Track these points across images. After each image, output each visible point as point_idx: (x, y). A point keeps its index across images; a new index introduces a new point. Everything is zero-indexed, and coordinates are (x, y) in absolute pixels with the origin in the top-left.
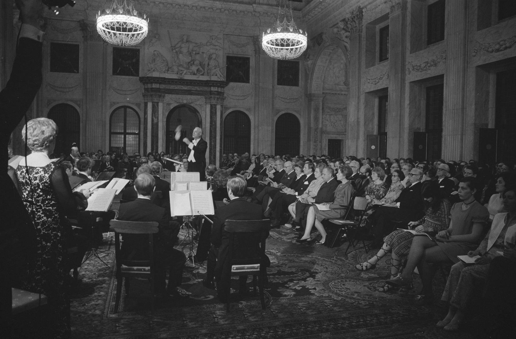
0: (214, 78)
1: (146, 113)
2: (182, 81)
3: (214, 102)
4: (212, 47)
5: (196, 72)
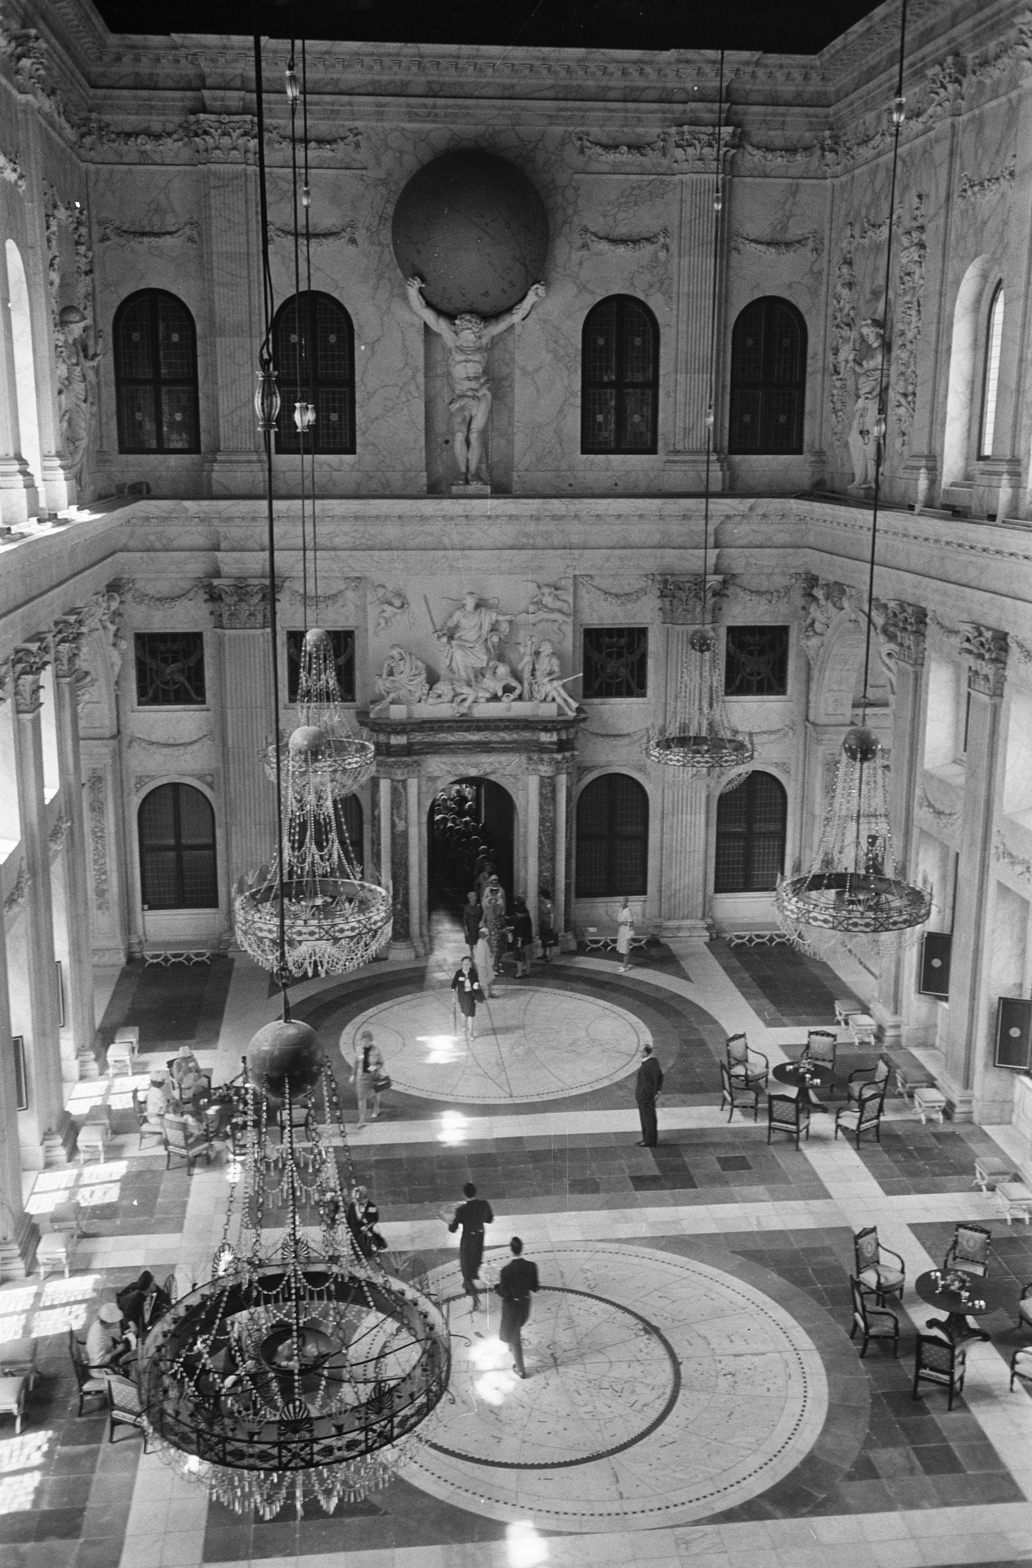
0: (548, 711)
1: (375, 804)
2: (466, 723)
3: (546, 770)
4: (545, 616)
5: (500, 693)
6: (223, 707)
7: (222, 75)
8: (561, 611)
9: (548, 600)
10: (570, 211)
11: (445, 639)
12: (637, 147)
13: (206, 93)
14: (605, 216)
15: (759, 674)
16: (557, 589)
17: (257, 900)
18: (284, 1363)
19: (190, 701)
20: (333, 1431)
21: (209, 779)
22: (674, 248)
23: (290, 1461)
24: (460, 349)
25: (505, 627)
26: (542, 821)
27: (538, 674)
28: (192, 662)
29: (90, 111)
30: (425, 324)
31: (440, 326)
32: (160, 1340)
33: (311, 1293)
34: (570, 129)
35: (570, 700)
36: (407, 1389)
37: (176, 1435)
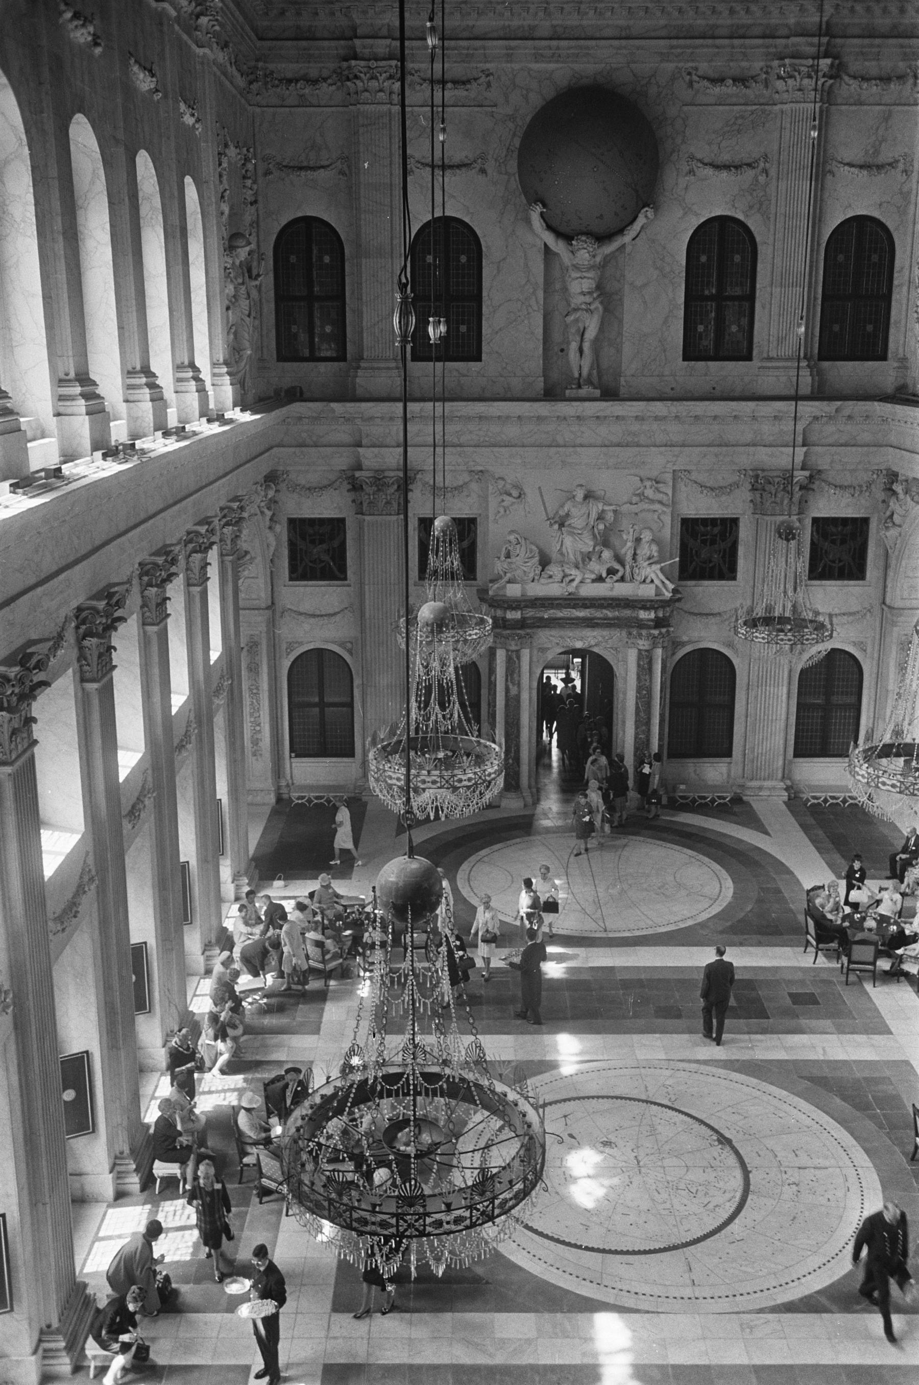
0: (647, 592)
1: (492, 671)
2: (573, 601)
3: (644, 644)
4: (646, 506)
5: (604, 575)
6: (361, 584)
7: (372, 25)
8: (660, 502)
9: (649, 493)
10: (679, 140)
11: (556, 526)
12: (741, 80)
13: (357, 42)
14: (710, 144)
15: (840, 561)
16: (657, 482)
17: (387, 752)
18: (403, 1148)
19: (333, 577)
20: (443, 1207)
21: (349, 645)
22: (773, 172)
23: (406, 1230)
24: (576, 267)
25: (610, 516)
26: (639, 689)
27: (639, 558)
28: (336, 543)
29: (257, 60)
30: (545, 244)
31: (558, 246)
32: (299, 1123)
33: (427, 1089)
34: (681, 65)
35: (667, 582)
36: (506, 1177)
37: (311, 1201)
